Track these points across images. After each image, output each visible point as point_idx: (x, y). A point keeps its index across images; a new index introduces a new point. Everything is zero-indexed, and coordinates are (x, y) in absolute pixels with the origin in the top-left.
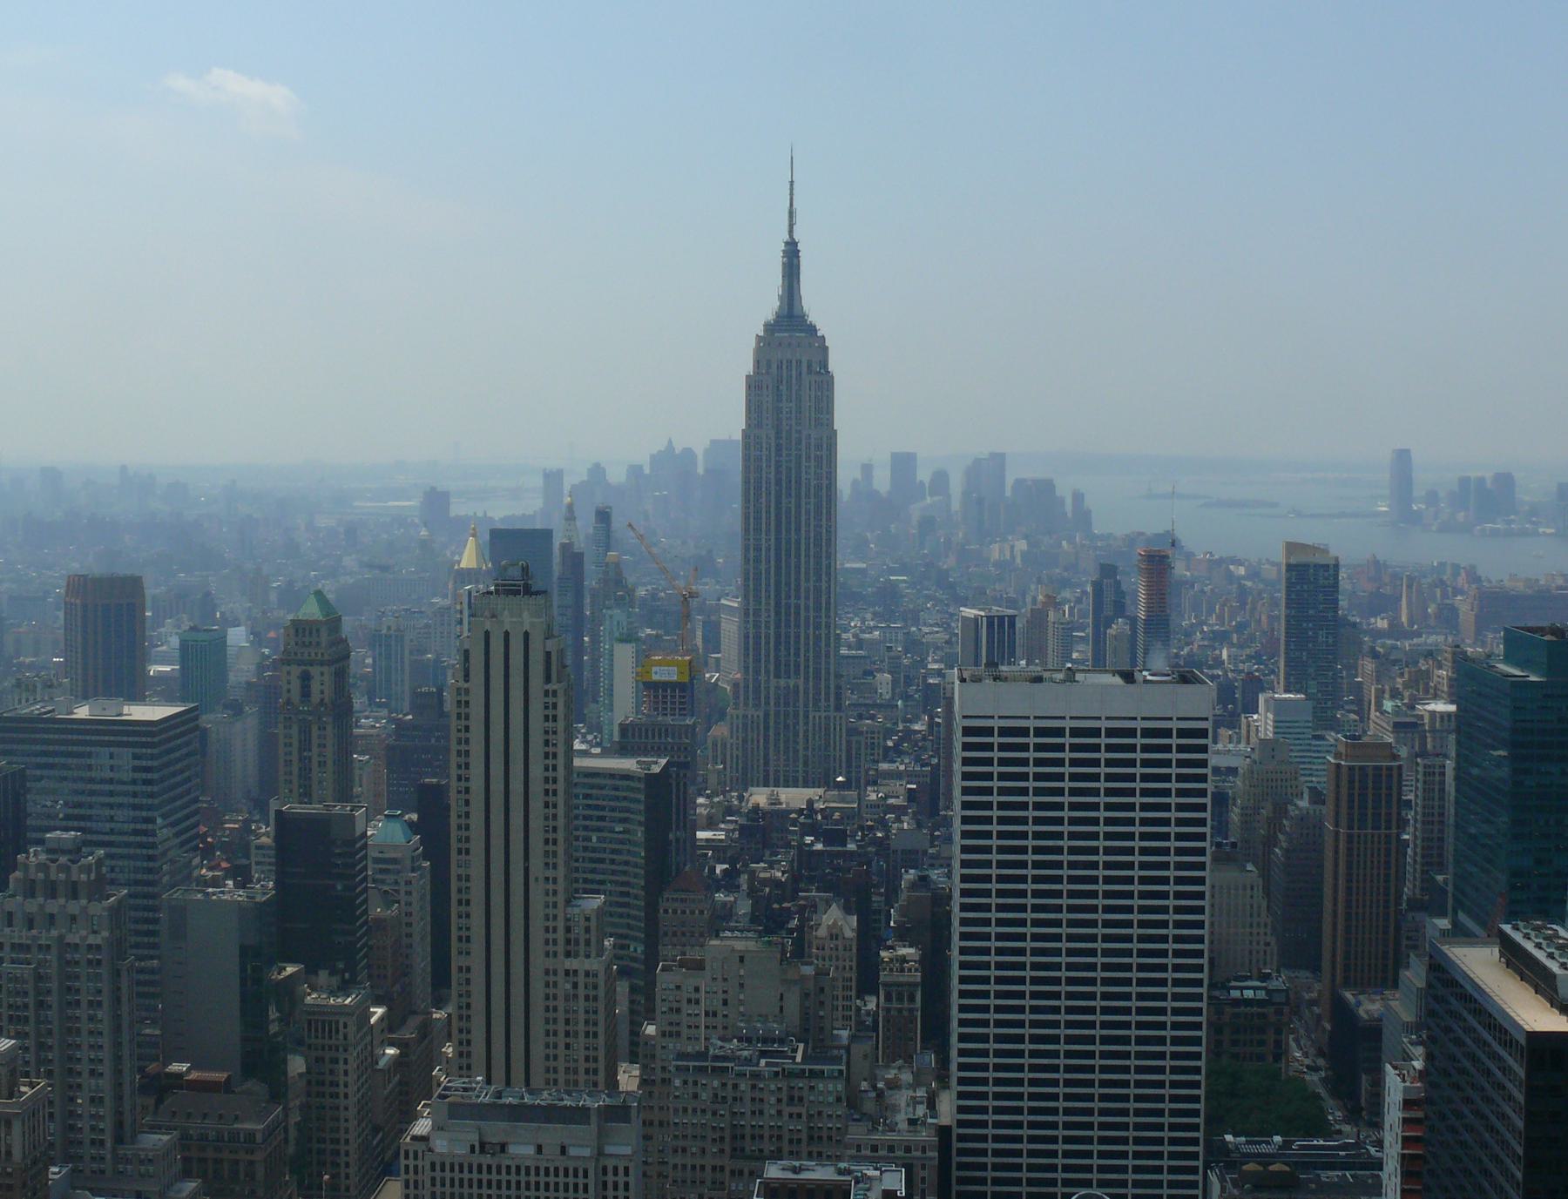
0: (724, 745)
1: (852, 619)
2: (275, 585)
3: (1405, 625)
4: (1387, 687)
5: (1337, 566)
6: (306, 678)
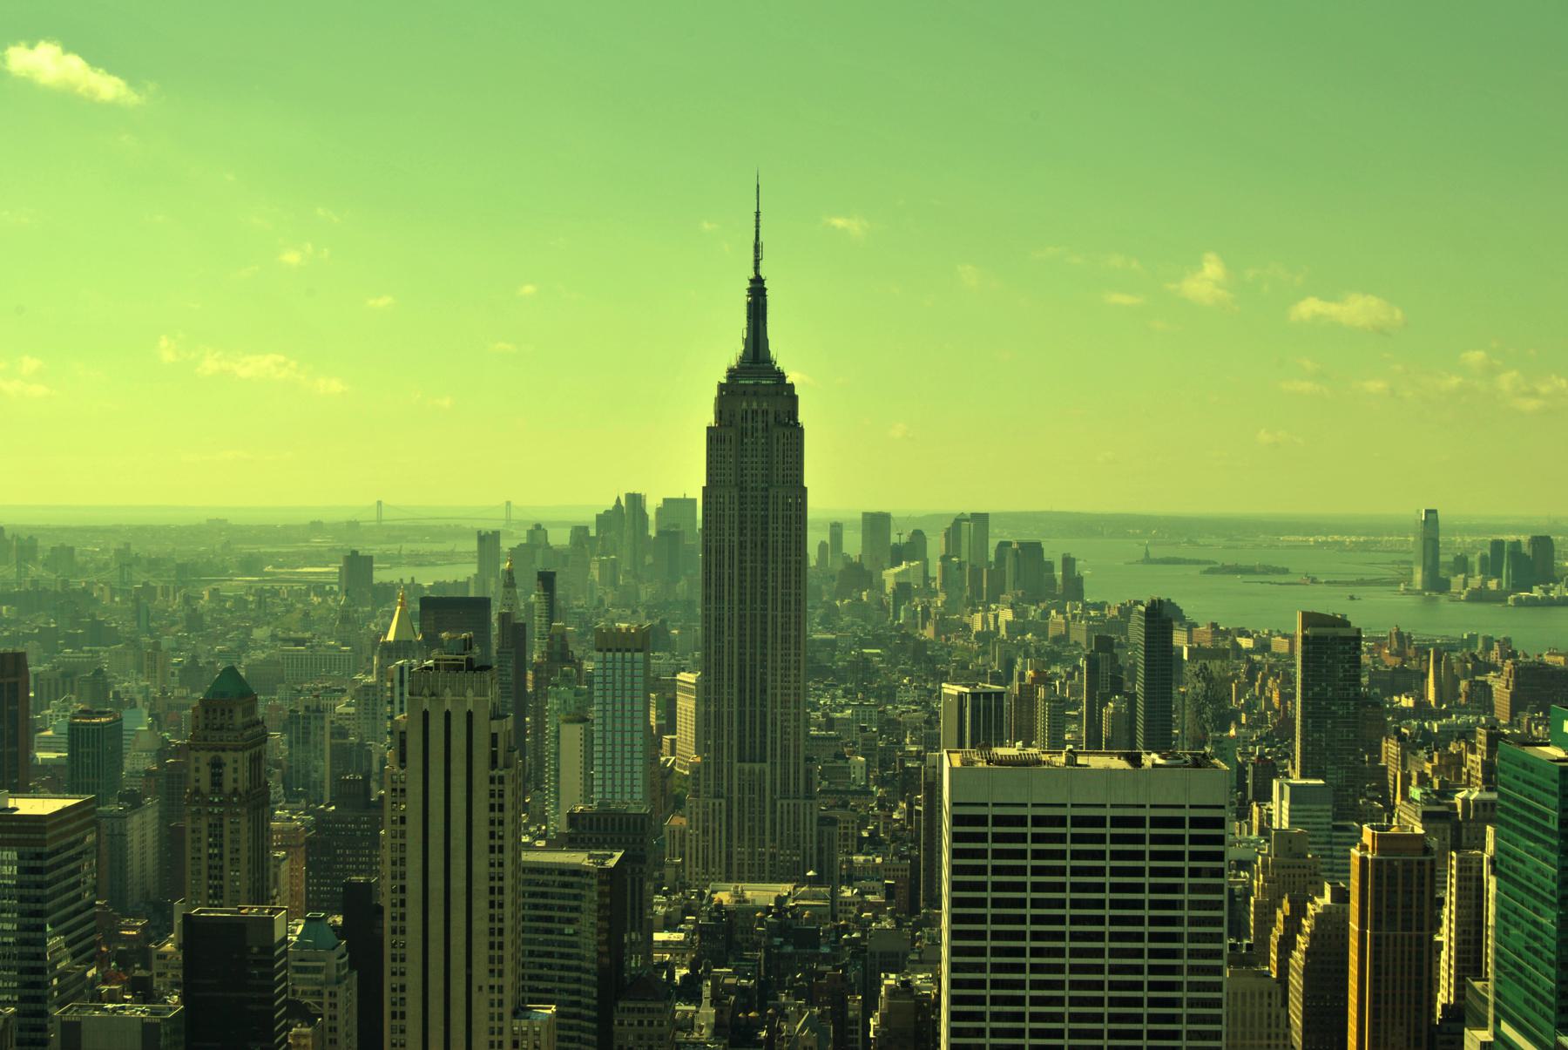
0: (683, 833)
1: (821, 696)
2: (175, 660)
3: (1433, 703)
4: (1414, 774)
5: (1357, 639)
6: (217, 765)
